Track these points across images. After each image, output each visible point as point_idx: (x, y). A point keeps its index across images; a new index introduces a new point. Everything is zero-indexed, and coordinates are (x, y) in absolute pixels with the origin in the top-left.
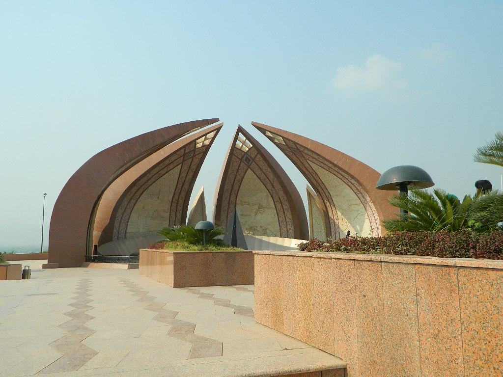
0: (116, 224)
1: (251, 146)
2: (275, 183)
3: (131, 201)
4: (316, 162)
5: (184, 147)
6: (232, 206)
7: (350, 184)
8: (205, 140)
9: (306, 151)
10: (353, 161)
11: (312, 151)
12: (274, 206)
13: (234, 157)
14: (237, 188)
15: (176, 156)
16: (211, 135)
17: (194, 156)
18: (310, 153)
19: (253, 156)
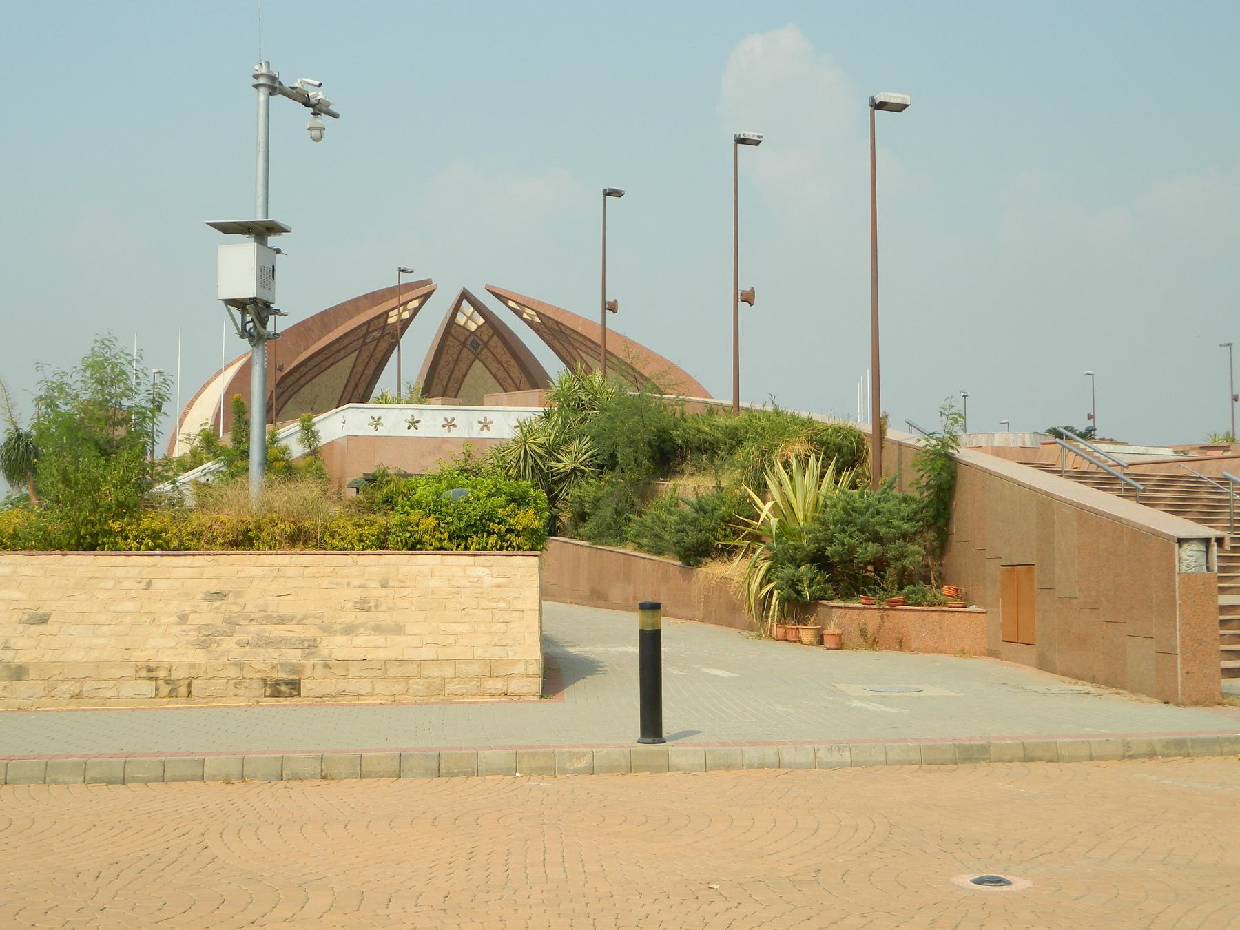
5: (368, 323)
8: (404, 310)
9: (575, 336)
10: (650, 356)
11: (585, 338)
13: (450, 338)
15: (352, 337)
16: (415, 303)
17: (383, 335)
18: (581, 339)
19: (485, 339)
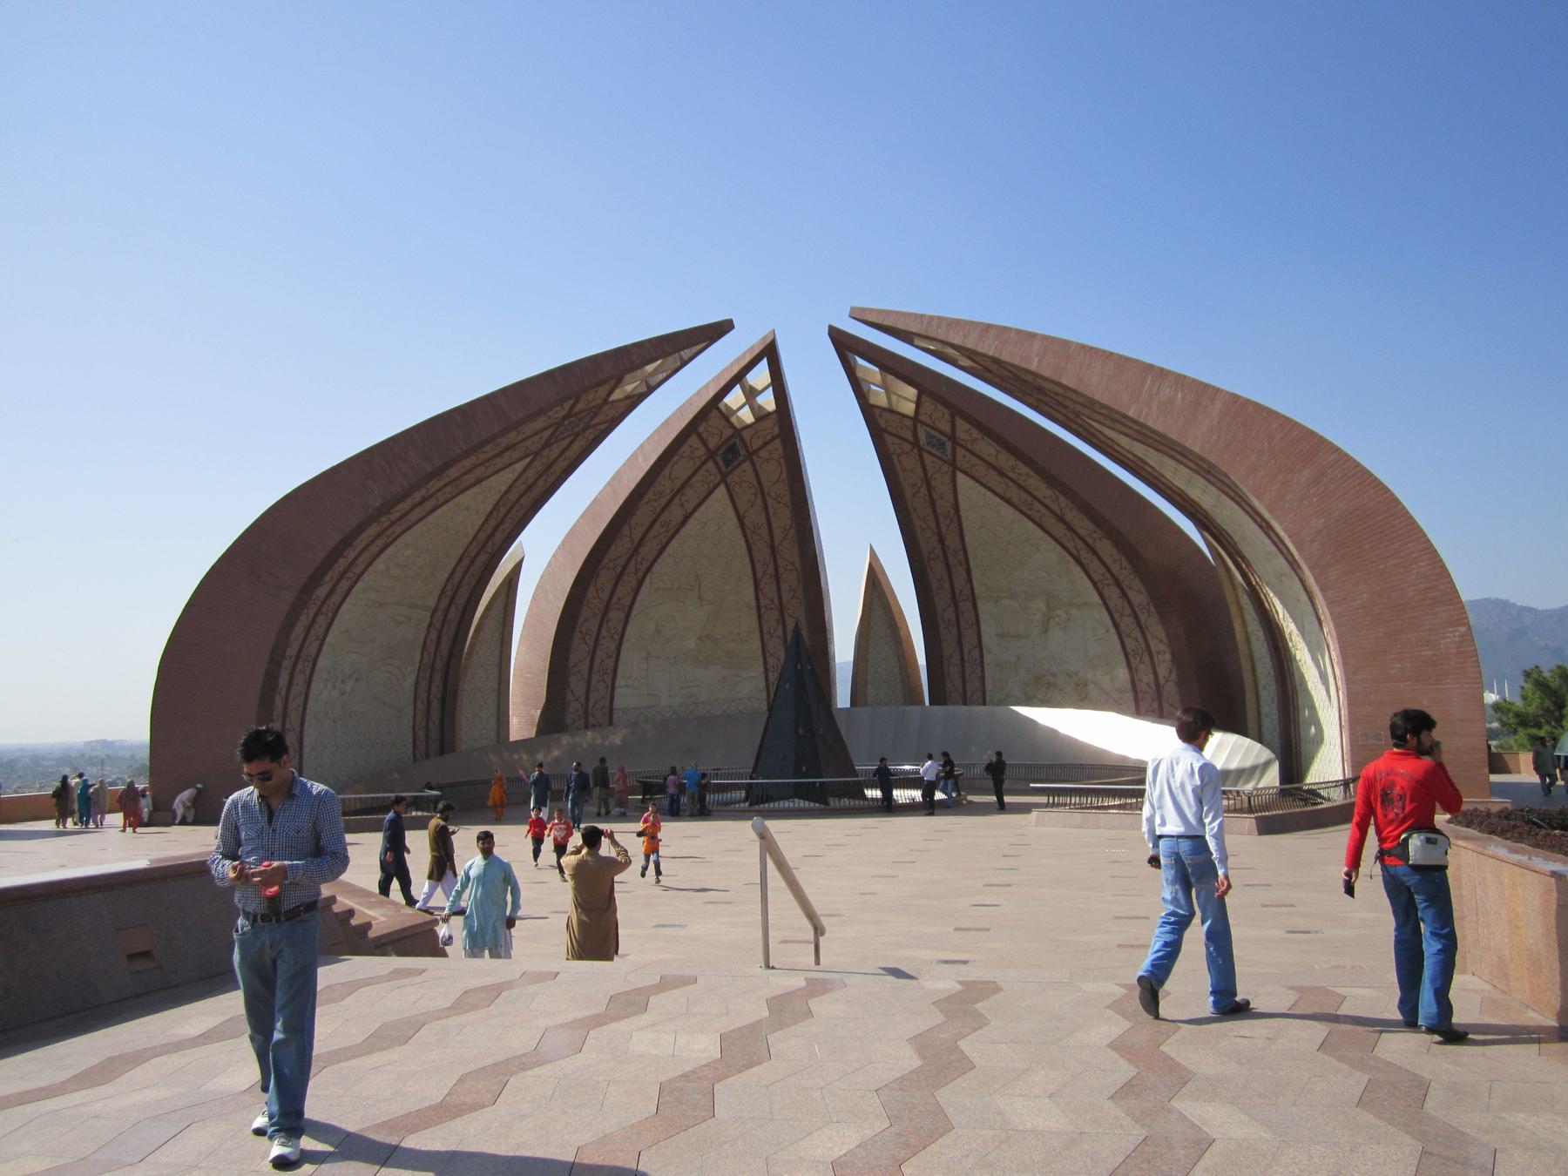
0: (577, 684)
1: (911, 392)
6: (965, 606)
12: (1096, 599)
13: (889, 439)
14: (958, 545)
16: (760, 376)
19: (946, 427)
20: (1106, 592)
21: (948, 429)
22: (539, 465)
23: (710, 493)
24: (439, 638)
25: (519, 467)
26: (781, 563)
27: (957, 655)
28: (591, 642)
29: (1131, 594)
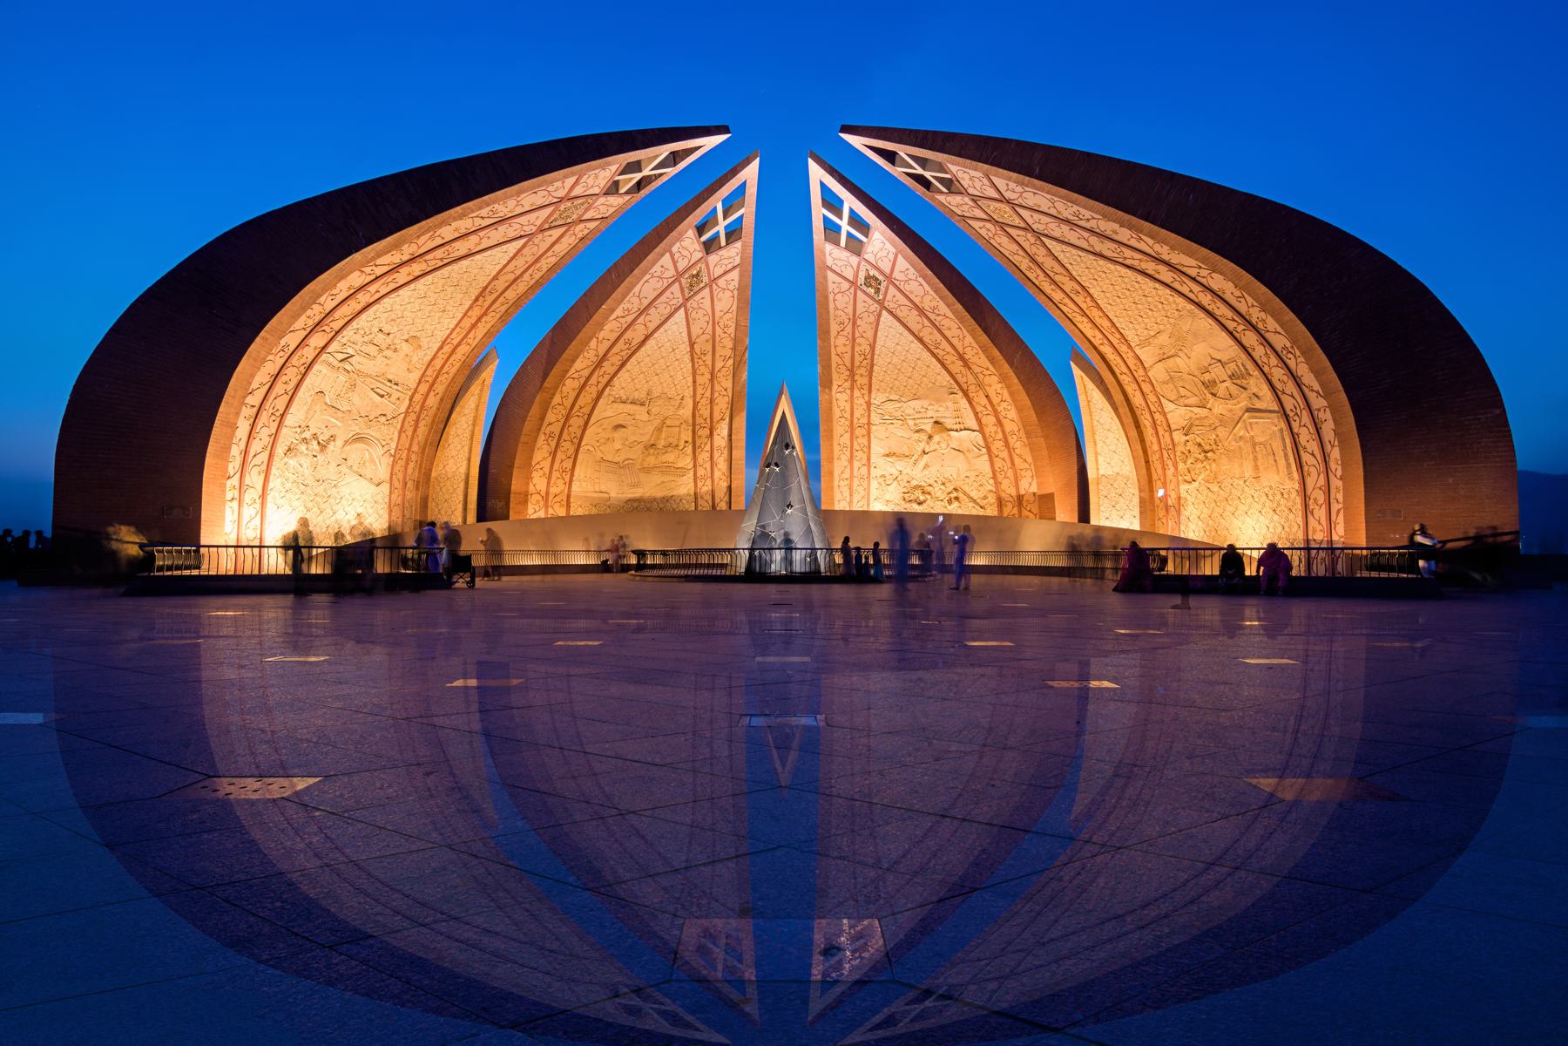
2: (968, 350)
3: (573, 421)
4: (1072, 236)
7: (1206, 299)
14: (865, 381)
19: (887, 268)
20: (984, 420)
21: (887, 270)
22: (529, 254)
23: (671, 315)
24: (417, 421)
25: (512, 248)
26: (717, 387)
27: (848, 471)
28: (553, 444)
29: (1005, 422)
